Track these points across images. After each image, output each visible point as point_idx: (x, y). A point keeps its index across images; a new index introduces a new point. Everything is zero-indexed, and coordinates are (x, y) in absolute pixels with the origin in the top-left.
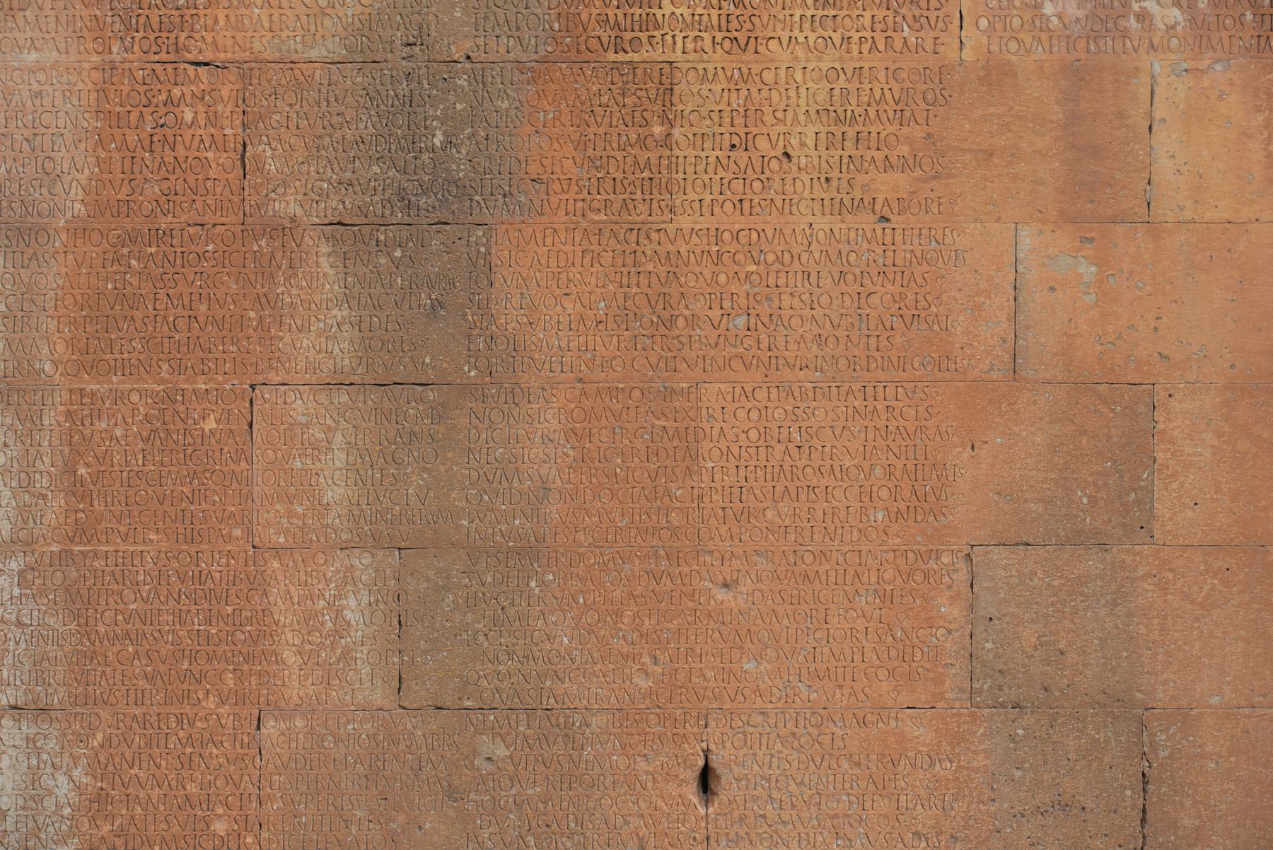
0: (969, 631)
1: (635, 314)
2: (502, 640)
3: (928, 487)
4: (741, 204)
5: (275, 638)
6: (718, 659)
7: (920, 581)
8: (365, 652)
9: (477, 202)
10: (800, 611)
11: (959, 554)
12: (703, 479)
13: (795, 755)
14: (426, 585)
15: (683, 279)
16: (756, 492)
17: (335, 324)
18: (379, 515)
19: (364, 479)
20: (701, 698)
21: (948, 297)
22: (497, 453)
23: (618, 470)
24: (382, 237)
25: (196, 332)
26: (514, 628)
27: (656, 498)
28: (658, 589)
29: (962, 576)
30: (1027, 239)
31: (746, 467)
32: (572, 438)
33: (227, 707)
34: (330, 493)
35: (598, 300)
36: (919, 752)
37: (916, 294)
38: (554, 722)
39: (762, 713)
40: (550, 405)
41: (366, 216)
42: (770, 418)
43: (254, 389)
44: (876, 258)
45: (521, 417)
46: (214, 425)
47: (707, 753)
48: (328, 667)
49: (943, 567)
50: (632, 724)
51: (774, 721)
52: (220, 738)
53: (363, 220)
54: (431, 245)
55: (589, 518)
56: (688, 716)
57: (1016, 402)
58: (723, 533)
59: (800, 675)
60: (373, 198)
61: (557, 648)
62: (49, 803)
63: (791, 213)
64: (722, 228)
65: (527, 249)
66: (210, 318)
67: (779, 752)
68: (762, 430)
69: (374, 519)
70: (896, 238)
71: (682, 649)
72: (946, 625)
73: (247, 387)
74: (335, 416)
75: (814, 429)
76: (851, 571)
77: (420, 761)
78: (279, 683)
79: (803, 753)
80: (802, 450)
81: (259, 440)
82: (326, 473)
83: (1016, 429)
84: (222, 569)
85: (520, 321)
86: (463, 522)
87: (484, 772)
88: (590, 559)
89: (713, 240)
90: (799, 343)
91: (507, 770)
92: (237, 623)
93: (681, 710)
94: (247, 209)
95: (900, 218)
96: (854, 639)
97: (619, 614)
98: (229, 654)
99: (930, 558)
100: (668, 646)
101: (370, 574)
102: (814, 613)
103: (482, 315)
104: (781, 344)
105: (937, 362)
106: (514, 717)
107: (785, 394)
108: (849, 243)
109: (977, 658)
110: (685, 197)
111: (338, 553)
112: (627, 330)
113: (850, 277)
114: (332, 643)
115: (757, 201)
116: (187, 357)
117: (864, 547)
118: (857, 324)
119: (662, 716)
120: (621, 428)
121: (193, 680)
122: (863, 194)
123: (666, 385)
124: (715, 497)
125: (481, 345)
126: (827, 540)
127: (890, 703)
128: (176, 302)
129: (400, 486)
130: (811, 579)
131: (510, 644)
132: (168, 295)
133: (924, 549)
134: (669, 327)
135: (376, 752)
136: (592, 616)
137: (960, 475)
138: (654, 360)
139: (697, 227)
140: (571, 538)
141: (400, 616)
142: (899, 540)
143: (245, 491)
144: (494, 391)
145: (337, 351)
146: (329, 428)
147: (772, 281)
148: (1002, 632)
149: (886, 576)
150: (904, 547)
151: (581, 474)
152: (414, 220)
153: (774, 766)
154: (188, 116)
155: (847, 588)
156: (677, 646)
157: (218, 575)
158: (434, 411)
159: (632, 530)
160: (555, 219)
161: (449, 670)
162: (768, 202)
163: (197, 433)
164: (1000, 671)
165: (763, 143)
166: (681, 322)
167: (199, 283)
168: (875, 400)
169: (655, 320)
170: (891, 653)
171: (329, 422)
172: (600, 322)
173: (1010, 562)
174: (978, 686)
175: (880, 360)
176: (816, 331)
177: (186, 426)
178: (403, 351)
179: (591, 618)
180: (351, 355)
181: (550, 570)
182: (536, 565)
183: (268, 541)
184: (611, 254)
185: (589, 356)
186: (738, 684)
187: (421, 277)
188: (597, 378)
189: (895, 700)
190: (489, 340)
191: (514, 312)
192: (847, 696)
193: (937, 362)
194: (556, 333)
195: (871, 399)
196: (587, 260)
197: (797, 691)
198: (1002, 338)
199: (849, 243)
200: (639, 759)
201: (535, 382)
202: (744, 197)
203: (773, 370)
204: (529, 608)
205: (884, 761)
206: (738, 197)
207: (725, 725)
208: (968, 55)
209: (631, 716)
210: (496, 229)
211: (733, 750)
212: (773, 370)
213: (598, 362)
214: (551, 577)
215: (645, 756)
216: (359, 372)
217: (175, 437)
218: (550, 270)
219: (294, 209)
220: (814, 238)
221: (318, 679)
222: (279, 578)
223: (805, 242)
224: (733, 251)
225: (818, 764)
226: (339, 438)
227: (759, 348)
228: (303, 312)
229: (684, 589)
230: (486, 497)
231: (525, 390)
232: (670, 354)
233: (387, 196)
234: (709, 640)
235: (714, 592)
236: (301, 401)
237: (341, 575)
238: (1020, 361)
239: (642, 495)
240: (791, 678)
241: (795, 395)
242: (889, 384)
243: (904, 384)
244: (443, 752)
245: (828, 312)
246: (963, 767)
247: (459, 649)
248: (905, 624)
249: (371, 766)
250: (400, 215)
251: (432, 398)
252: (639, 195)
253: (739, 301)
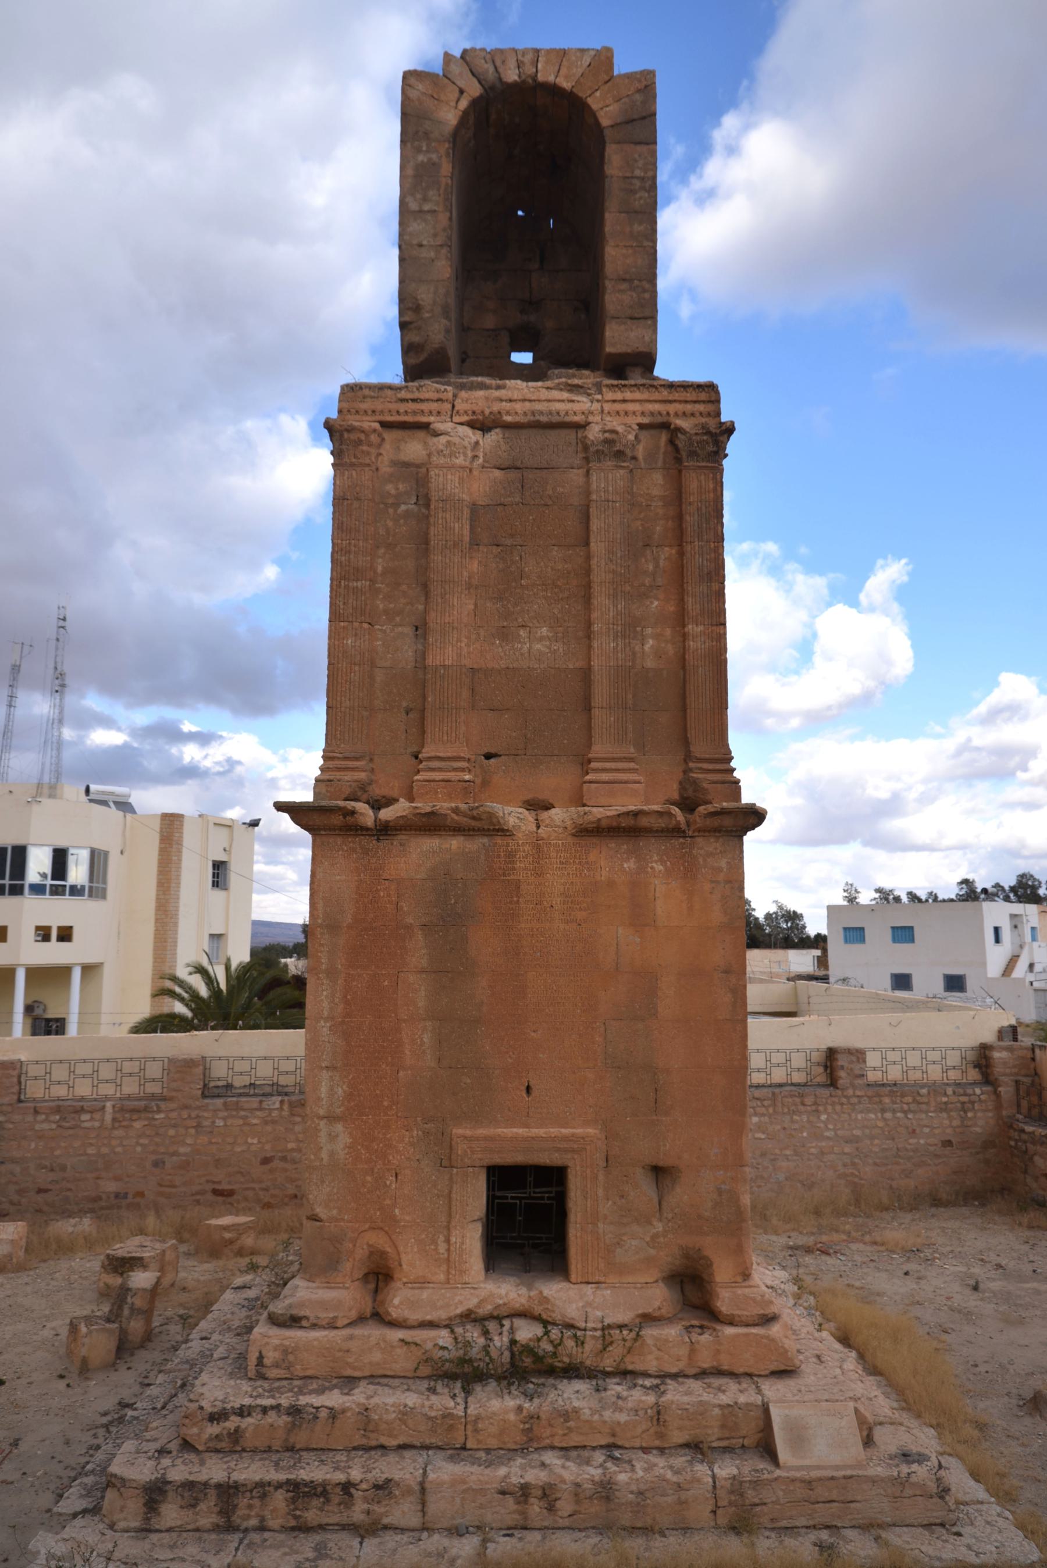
29: (602, 1029)
30: (620, 930)
62: (336, 1096)
154: (382, 894)
165: (545, 903)
208: (603, 878)
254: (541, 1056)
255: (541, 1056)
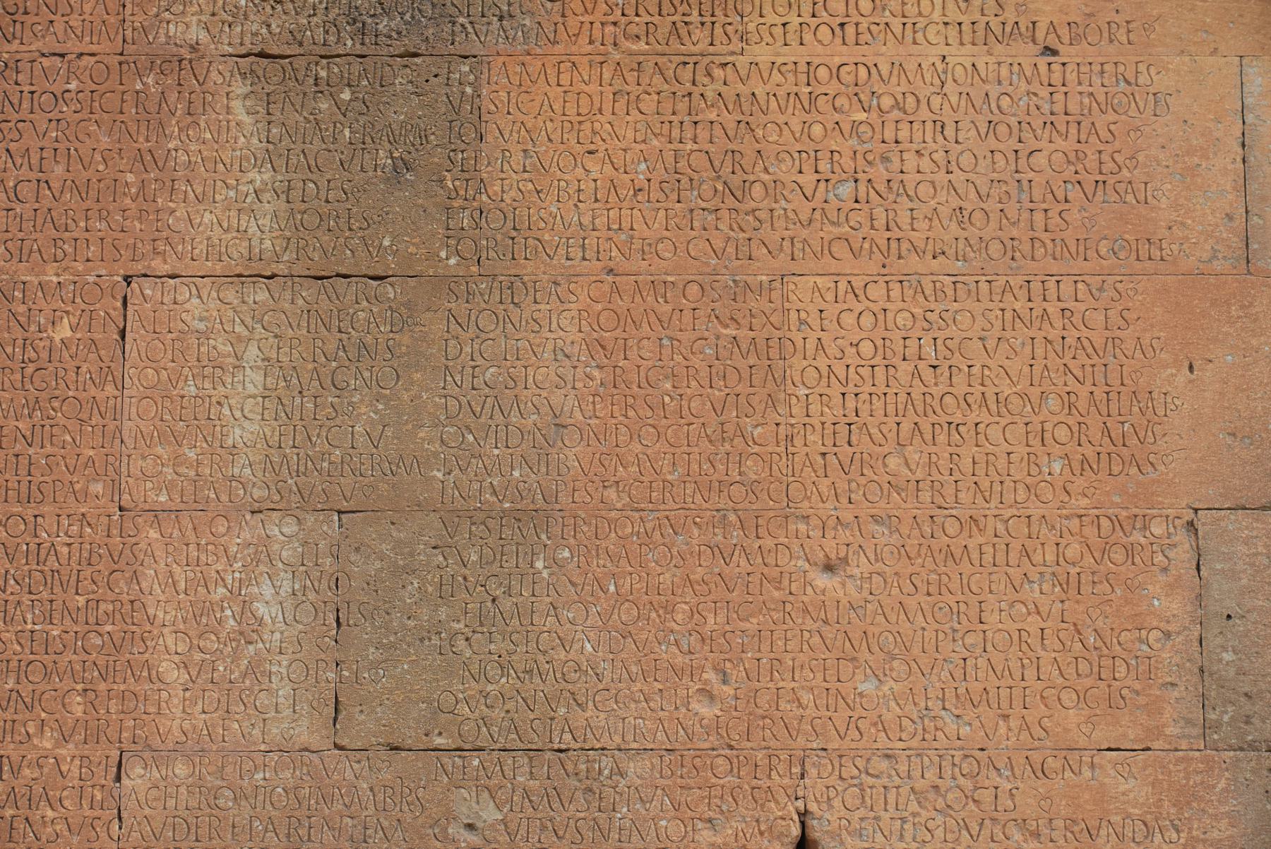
0: (1197, 634)
1: (691, 180)
2: (492, 647)
3: (1126, 425)
4: (843, 30)
5: (148, 643)
6: (820, 676)
7: (1120, 562)
8: (285, 663)
9: (462, 25)
10: (942, 605)
11: (1177, 522)
12: (794, 412)
13: (940, 819)
14: (378, 565)
15: (760, 133)
16: (872, 431)
17: (252, 191)
18: (310, 463)
19: (289, 410)
20: (794, 733)
21: (1147, 156)
22: (488, 375)
23: (667, 399)
24: (323, 74)
25: (47, 202)
26: (510, 629)
27: (723, 438)
28: (727, 570)
31: (856, 395)
32: (598, 352)
33: (71, 746)
34: (238, 431)
35: (636, 160)
36: (1129, 816)
37: (1100, 152)
38: (570, 767)
39: (888, 756)
40: (567, 306)
41: (301, 44)
42: (891, 325)
43: (129, 284)
44: (1040, 103)
45: (524, 323)
46: (69, 333)
47: (804, 815)
48: (228, 686)
49: (1156, 540)
50: (689, 772)
51: (906, 768)
52: (58, 794)
53: (295, 50)
54: (394, 84)
55: (624, 467)
56: (775, 761)
57: (1251, 304)
58: (824, 489)
59: (943, 700)
60: (311, 19)
61: (576, 659)
63: (915, 43)
64: (816, 61)
65: (533, 89)
66: (69, 182)
67: (914, 815)
68: (879, 343)
69: (302, 469)
70: (1068, 75)
71: (764, 661)
72: (1162, 625)
73: (120, 279)
74: (248, 321)
75: (956, 341)
76: (1016, 546)
77: (366, 828)
78: (152, 710)
79: (951, 816)
80: (939, 371)
81: (135, 354)
82: (232, 402)
83: (1254, 342)
84: (72, 540)
85: (523, 189)
86: (435, 472)
87: (463, 845)
88: (625, 526)
89: (803, 78)
90: (930, 220)
91: (498, 842)
92: (92, 620)
93: (764, 752)
94: (129, 33)
95: (1073, 50)
96: (1024, 647)
97: (669, 609)
98: (78, 667)
99: (1134, 528)
100: (744, 655)
101: (295, 549)
102: (963, 607)
103: (467, 180)
104: (904, 219)
105: (1134, 247)
106: (510, 762)
107: (911, 292)
108: (1000, 83)
109: (1211, 675)
110: (762, 20)
111: (248, 517)
112: (679, 202)
113: (1002, 129)
114: (235, 650)
115: (866, 25)
116: (33, 237)
117: (1036, 511)
118: (1014, 193)
119: (735, 760)
120: (671, 339)
121: (21, 706)
122: (1018, 16)
123: (737, 278)
124: (811, 438)
125: (466, 221)
126: (979, 500)
127: (1083, 741)
128: (19, 161)
129: (343, 421)
130: (957, 557)
131: (504, 653)
132: (8, 150)
133: (1124, 513)
134: (740, 198)
135: (297, 813)
136: (628, 611)
137: (1173, 407)
138: (718, 244)
139: (780, 60)
140: (597, 496)
141: (338, 610)
142: (1086, 501)
143: (112, 426)
144: (484, 286)
145: (253, 229)
146: (239, 338)
147: (889, 135)
148: (1247, 636)
149: (1069, 553)
150: (1096, 512)
151: (613, 404)
152: (371, 50)
153: (908, 837)
155: (1010, 571)
156: (758, 655)
157: (65, 550)
158: (395, 314)
159: (688, 485)
160: (574, 49)
161: (411, 691)
162: (882, 27)
163: (42, 344)
164: (1246, 695)
166: (757, 190)
167: (54, 134)
168: (1045, 300)
169: (720, 188)
170: (1080, 666)
171: (239, 329)
172: (640, 190)
173: (1255, 533)
174: (1213, 717)
175: (1050, 245)
176: (956, 202)
177: (26, 335)
178: (350, 229)
179: (627, 613)
180: (274, 235)
181: (565, 542)
182: (544, 537)
183: (143, 499)
184: (656, 97)
185: (623, 237)
186: (851, 714)
187: (378, 127)
188: (634, 268)
189: (1089, 737)
190: (476, 214)
191: (514, 175)
192: (1016, 731)
193: (1134, 247)
194: (576, 205)
195: (1038, 299)
196: (621, 106)
197: (940, 724)
198: (1227, 215)
199: (1000, 83)
200: (700, 825)
201: (544, 273)
202: (847, 20)
203: (893, 257)
204: (534, 599)
205: (1076, 829)
206: (839, 20)
207: (831, 774)
209: (687, 760)
210: (489, 63)
211: (843, 812)
212: (893, 257)
213: (637, 244)
214: (566, 554)
215: (710, 821)
216: (285, 258)
217: (9, 350)
218: (567, 118)
219: (197, 33)
220: (949, 76)
221: (211, 703)
222: (157, 553)
223: (937, 82)
224: (832, 93)
225: (974, 833)
226: (253, 351)
227: (872, 227)
228: (205, 175)
229: (766, 571)
230: (471, 438)
231: (529, 285)
232: (742, 235)
233: (331, 16)
234: (805, 647)
235: (811, 575)
236: (198, 300)
237: (251, 550)
238: (1256, 246)
239: (703, 434)
240: (930, 704)
241: (927, 292)
242: (1064, 278)
243: (1085, 278)
244: (400, 814)
245: (972, 176)
246: (1197, 840)
247: (427, 659)
248: (1100, 623)
249: (288, 836)
250: (349, 43)
251: (392, 296)
252: (695, 17)
253: (841, 161)
254: (868, 687)
255: (868, 687)
